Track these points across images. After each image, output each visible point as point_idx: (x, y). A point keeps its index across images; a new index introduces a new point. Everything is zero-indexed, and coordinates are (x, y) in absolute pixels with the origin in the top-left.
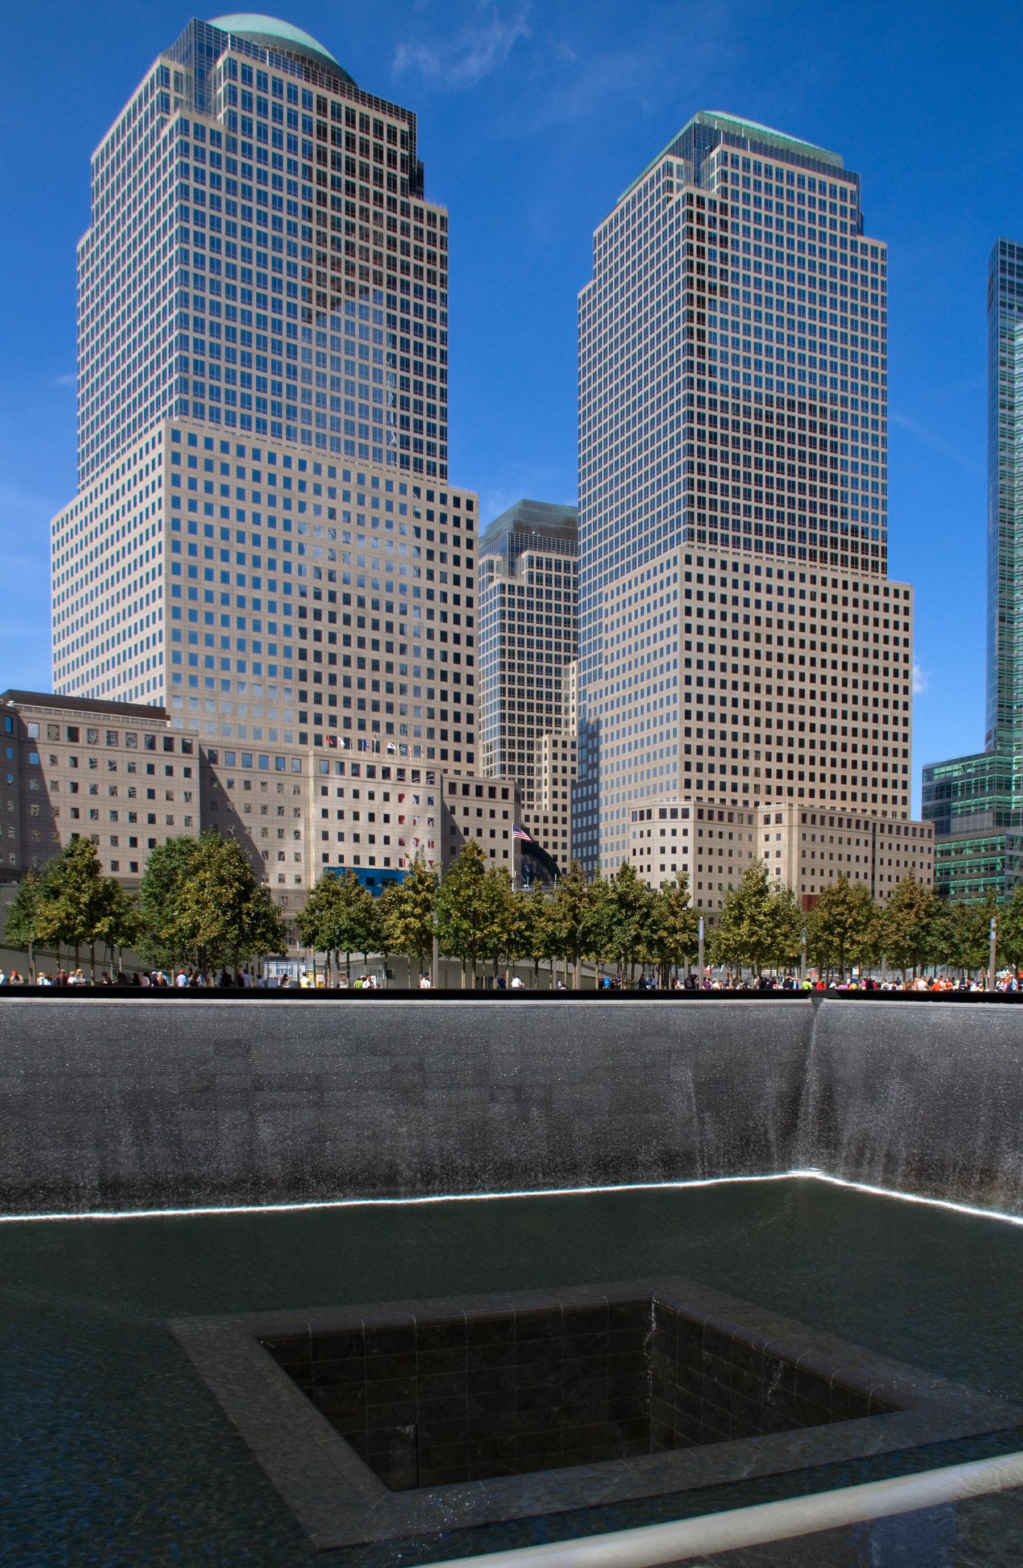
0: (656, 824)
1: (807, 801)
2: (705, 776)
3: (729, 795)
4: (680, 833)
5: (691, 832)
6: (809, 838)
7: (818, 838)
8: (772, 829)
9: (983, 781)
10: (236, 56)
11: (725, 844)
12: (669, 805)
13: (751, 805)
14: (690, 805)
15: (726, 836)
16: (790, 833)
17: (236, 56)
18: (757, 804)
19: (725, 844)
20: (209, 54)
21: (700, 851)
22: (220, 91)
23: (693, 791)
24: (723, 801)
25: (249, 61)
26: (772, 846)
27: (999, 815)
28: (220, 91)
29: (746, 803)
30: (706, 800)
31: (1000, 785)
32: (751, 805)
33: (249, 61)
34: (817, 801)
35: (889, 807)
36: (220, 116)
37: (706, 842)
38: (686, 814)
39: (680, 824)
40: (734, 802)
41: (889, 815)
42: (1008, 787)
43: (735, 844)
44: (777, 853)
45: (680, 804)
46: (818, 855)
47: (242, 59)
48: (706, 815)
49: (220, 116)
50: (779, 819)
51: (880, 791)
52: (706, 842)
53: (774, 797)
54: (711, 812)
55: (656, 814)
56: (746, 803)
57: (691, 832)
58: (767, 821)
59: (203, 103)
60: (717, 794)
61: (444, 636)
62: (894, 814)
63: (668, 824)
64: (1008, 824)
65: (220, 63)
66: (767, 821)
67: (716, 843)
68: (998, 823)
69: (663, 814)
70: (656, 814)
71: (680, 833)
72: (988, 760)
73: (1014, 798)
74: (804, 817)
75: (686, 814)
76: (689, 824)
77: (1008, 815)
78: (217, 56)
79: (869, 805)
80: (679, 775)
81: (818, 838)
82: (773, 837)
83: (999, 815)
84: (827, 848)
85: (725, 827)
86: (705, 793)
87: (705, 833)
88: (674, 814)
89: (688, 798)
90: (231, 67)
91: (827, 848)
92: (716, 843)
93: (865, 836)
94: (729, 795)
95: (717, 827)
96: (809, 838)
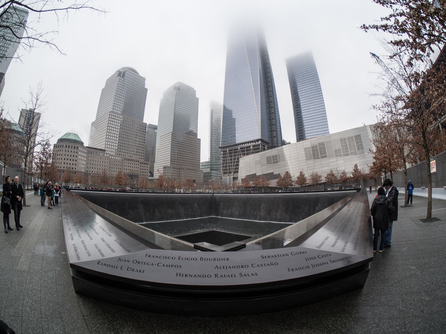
8: (182, 170)
84: (190, 173)
91: (190, 173)
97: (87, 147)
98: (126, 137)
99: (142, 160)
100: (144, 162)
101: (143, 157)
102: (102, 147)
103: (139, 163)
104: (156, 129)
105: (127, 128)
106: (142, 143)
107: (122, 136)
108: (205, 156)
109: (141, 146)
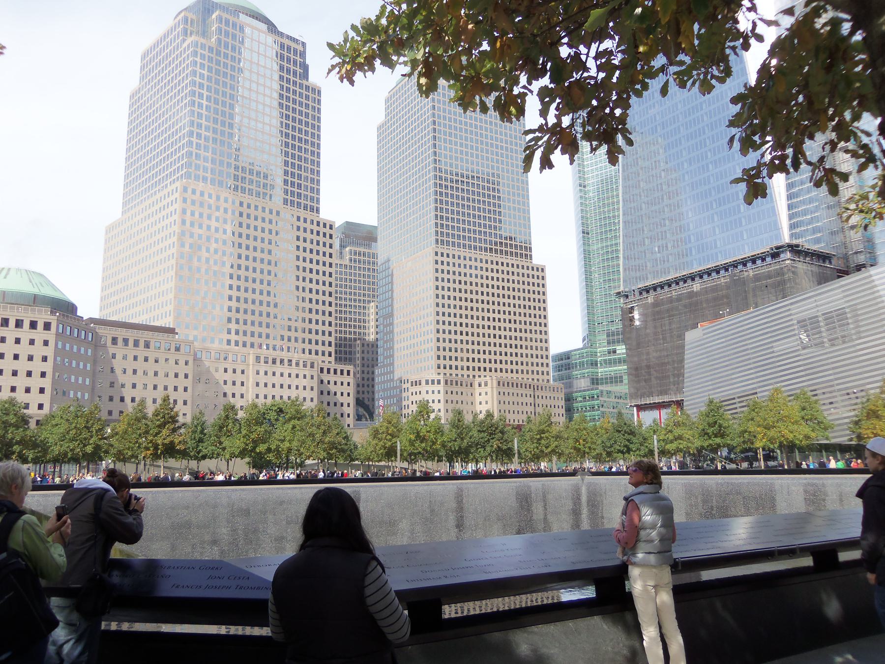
0: (424, 388)
1: (499, 374)
2: (448, 363)
3: (459, 372)
4: (436, 392)
5: (442, 392)
6: (502, 394)
7: (506, 394)
8: (483, 390)
9: (583, 362)
10: (222, 14)
11: (459, 398)
12: (430, 378)
13: (471, 377)
14: (441, 377)
15: (459, 393)
16: (492, 391)
17: (222, 14)
18: (474, 376)
19: (459, 398)
20: (209, 12)
21: (447, 401)
22: (214, 28)
23: (442, 370)
24: (457, 375)
25: (228, 17)
26: (483, 398)
27: (593, 379)
28: (214, 28)
29: (468, 376)
30: (448, 375)
31: (592, 364)
32: (471, 377)
33: (228, 17)
34: (504, 374)
35: (540, 377)
36: (213, 40)
37: (450, 397)
38: (439, 382)
39: (436, 387)
40: (463, 376)
41: (541, 381)
42: (596, 365)
43: (463, 398)
44: (484, 401)
45: (436, 377)
46: (507, 403)
47: (225, 16)
48: (449, 382)
49: (213, 40)
50: (486, 385)
51: (535, 368)
52: (450, 397)
53: (482, 373)
54: (452, 381)
55: (423, 382)
56: (468, 376)
57: (442, 392)
58: (480, 385)
59: (204, 34)
60: (454, 372)
61: (311, 291)
62: (543, 381)
63: (430, 388)
64: (597, 384)
65: (214, 16)
66: (480, 385)
67: (454, 397)
68: (593, 383)
69: (427, 382)
70: (423, 382)
71: (436, 392)
72: (585, 351)
73: (600, 370)
74: (499, 382)
75: (439, 382)
76: (441, 387)
77: (597, 379)
78: (213, 13)
79: (530, 376)
80: (434, 362)
81: (506, 394)
82: (483, 394)
83: (593, 379)
84: (511, 399)
85: (459, 389)
86: (448, 371)
87: (449, 392)
88: (433, 381)
89: (439, 374)
90: (220, 19)
91: (511, 399)
92: (454, 397)
93: (530, 392)
94: (459, 372)
95: (455, 389)
96: (502, 394)
97: (92, 320)
98: (258, 275)
99: (327, 358)
100: (333, 366)
101: (327, 349)
102: (167, 322)
103: (315, 372)
104: (375, 240)
105: (258, 244)
106: (321, 297)
107: (242, 273)
108: (566, 328)
109: (320, 307)
